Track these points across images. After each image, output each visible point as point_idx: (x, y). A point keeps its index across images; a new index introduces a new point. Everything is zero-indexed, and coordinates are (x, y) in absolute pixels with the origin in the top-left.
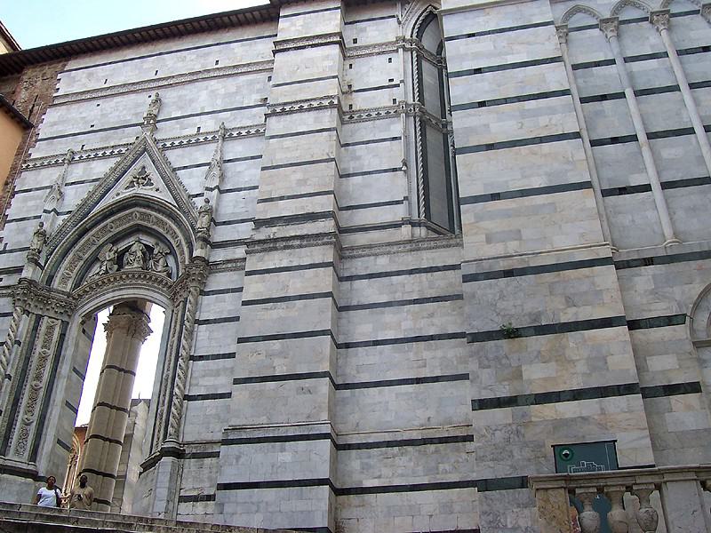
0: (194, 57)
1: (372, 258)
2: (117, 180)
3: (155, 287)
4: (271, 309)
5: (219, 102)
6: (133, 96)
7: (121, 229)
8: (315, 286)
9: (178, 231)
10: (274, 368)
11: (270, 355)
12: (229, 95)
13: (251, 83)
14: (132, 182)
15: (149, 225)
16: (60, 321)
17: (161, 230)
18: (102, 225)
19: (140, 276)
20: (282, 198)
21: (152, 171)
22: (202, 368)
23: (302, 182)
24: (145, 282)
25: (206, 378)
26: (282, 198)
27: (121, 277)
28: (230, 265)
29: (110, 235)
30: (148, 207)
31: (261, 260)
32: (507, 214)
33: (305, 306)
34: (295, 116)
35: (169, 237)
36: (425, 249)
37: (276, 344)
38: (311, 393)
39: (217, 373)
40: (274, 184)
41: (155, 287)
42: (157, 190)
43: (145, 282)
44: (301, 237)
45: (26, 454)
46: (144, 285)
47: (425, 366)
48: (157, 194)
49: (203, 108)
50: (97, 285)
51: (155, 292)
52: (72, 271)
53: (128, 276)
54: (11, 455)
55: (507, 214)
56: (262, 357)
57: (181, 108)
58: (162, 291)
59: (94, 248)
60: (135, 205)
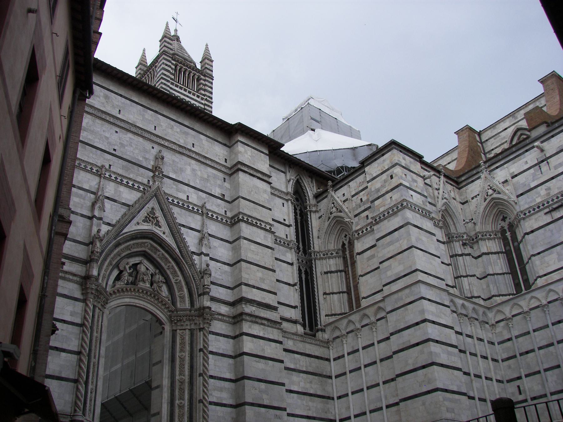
0: (178, 130)
1: (286, 339)
2: (139, 212)
3: (158, 306)
4: (258, 362)
5: (198, 181)
6: (141, 139)
7: (135, 250)
8: (277, 354)
9: (179, 273)
10: (263, 399)
11: (260, 391)
12: (202, 179)
13: (215, 177)
14: (146, 217)
15: (155, 256)
16: (101, 312)
17: (163, 264)
18: (128, 244)
19: (151, 295)
20: (254, 287)
21: (159, 213)
22: (213, 384)
23: (262, 280)
24: (152, 300)
25: (216, 392)
26: (254, 287)
27: (138, 290)
28: (220, 317)
29: (129, 252)
30: (160, 245)
31: (250, 327)
32: (451, 401)
33: (273, 365)
34: (255, 229)
35: (168, 272)
36: (309, 343)
37: (263, 385)
38: (280, 419)
39: (221, 390)
40: (249, 274)
41: (158, 306)
42: (164, 233)
43: (152, 300)
44: (268, 320)
45: (91, 415)
46: (151, 302)
47: (310, 410)
48: (164, 236)
49: (189, 180)
50: (122, 290)
51: (158, 309)
52: (106, 272)
53: (143, 291)
54: (87, 417)
55: (451, 401)
56: (257, 391)
57: (175, 172)
58: (163, 310)
59: (119, 258)
60: (152, 239)
